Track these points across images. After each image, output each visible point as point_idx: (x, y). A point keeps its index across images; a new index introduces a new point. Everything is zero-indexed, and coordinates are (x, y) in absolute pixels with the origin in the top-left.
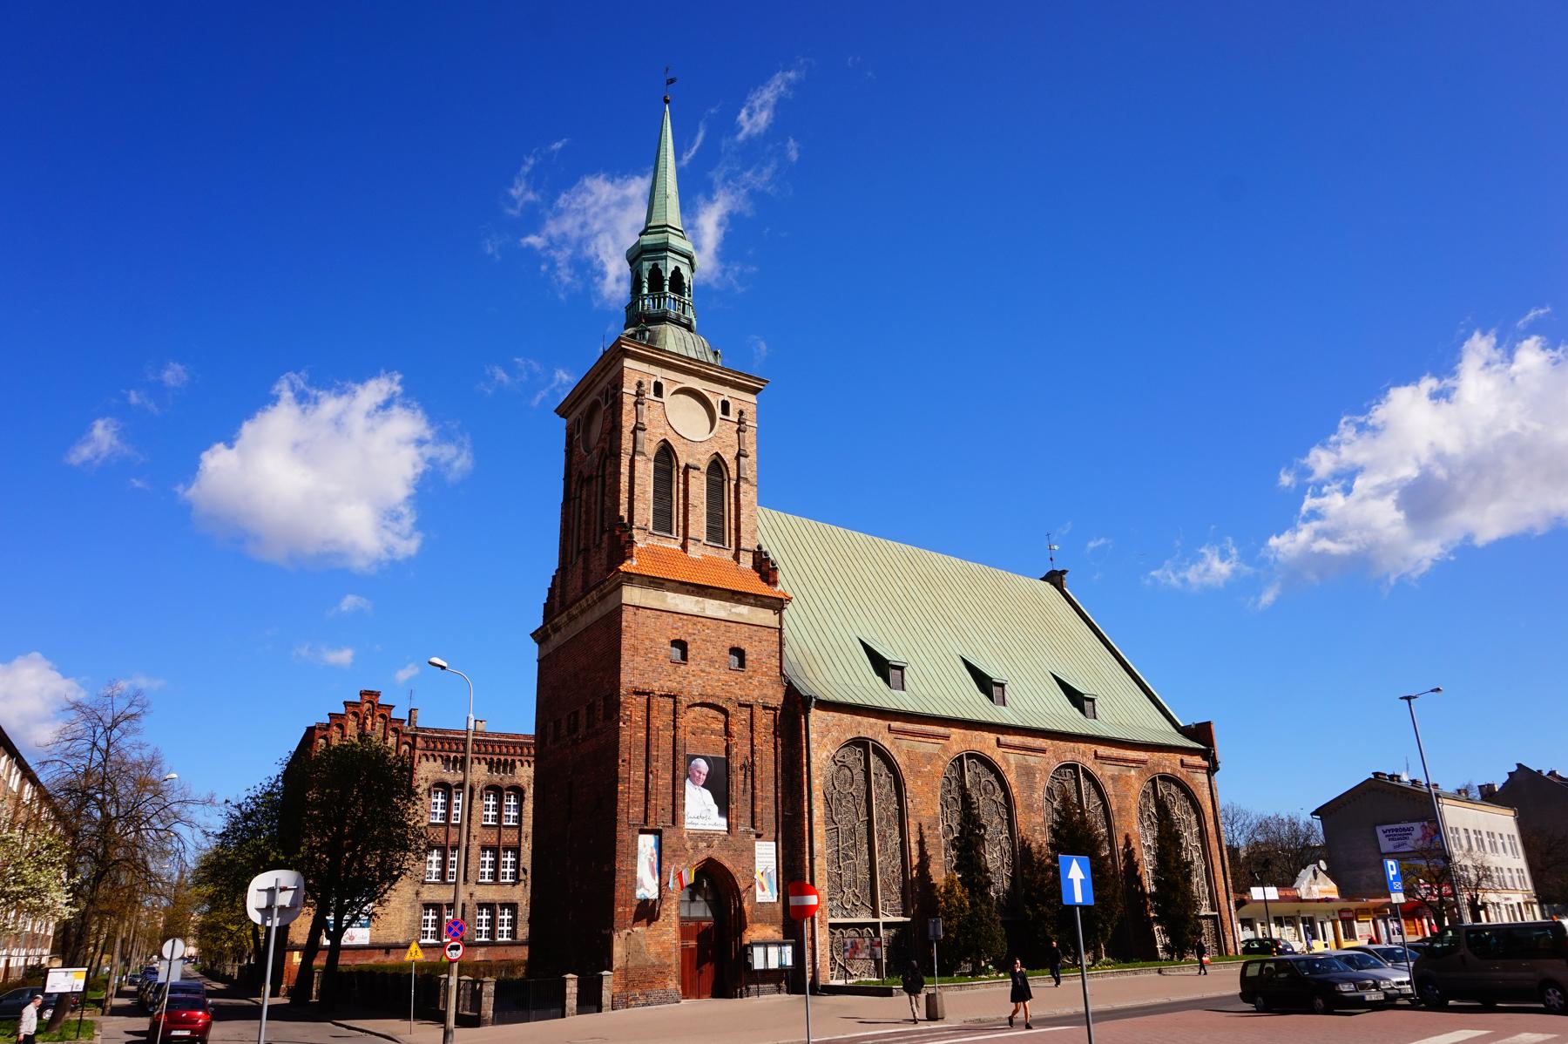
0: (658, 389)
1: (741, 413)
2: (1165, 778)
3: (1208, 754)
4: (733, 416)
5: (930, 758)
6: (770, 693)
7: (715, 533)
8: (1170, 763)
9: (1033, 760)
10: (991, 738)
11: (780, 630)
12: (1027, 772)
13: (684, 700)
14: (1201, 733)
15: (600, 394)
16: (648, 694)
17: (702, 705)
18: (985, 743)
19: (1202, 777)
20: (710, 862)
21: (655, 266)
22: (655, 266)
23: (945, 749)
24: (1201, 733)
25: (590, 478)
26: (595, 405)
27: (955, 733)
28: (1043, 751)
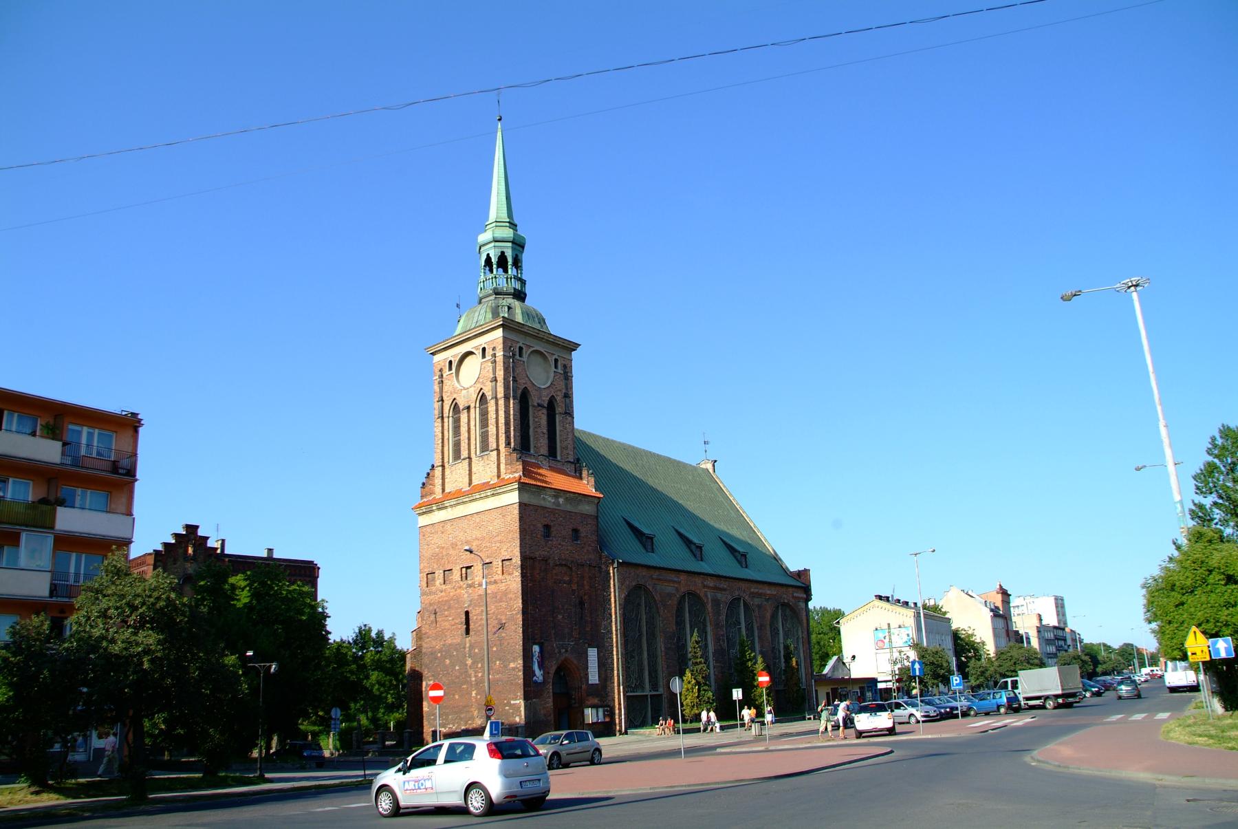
0: (521, 349)
1: (565, 366)
2: (784, 605)
3: (807, 591)
4: (560, 370)
5: (670, 595)
6: (592, 556)
7: (552, 452)
8: (787, 597)
9: (719, 595)
10: (698, 580)
11: (597, 517)
12: (716, 603)
13: (551, 562)
14: (803, 575)
15: (476, 348)
16: (533, 559)
17: (561, 565)
18: (697, 585)
19: (802, 605)
20: (566, 660)
21: (503, 253)
22: (503, 253)
23: (677, 590)
24: (803, 575)
25: (468, 408)
26: (470, 353)
27: (683, 577)
28: (725, 590)
